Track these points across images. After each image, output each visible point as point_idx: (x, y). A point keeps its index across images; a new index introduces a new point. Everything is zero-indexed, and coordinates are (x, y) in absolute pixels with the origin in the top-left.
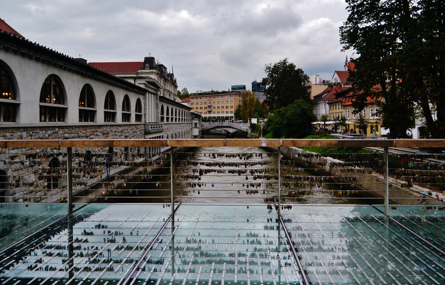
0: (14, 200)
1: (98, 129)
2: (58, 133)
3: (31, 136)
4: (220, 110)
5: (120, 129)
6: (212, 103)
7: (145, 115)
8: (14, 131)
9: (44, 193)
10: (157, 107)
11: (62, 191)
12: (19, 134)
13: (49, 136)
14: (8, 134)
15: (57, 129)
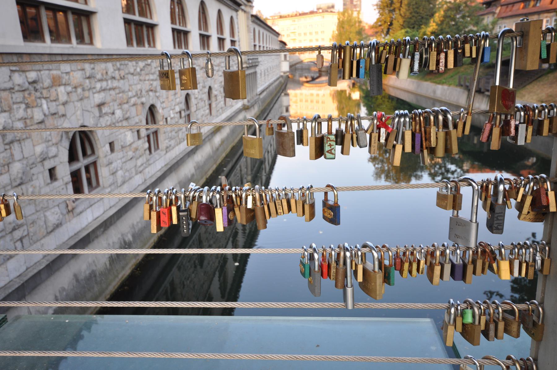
0: (111, 172)
2: (151, 66)
3: (119, 69)
9: (146, 159)
10: (249, 31)
11: (165, 154)
14: (87, 66)
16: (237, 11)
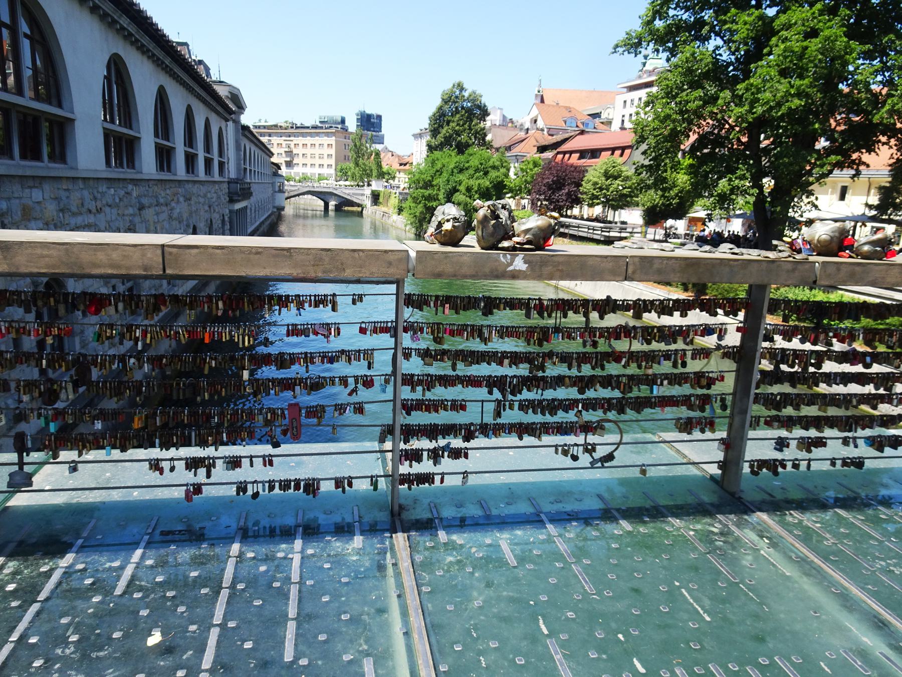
1: (180, 190)
3: (95, 199)
4: (309, 161)
5: (203, 189)
6: (292, 146)
7: (228, 163)
8: (71, 187)
12: (78, 194)
13: (120, 200)
15: (130, 187)
16: (227, 120)
